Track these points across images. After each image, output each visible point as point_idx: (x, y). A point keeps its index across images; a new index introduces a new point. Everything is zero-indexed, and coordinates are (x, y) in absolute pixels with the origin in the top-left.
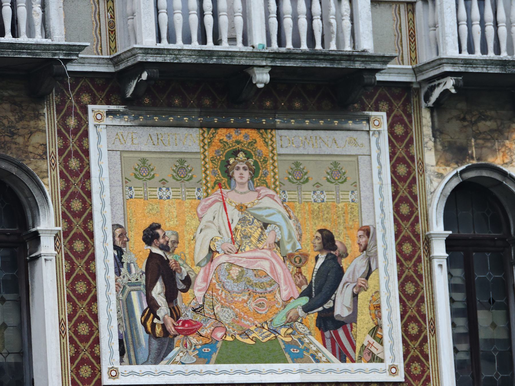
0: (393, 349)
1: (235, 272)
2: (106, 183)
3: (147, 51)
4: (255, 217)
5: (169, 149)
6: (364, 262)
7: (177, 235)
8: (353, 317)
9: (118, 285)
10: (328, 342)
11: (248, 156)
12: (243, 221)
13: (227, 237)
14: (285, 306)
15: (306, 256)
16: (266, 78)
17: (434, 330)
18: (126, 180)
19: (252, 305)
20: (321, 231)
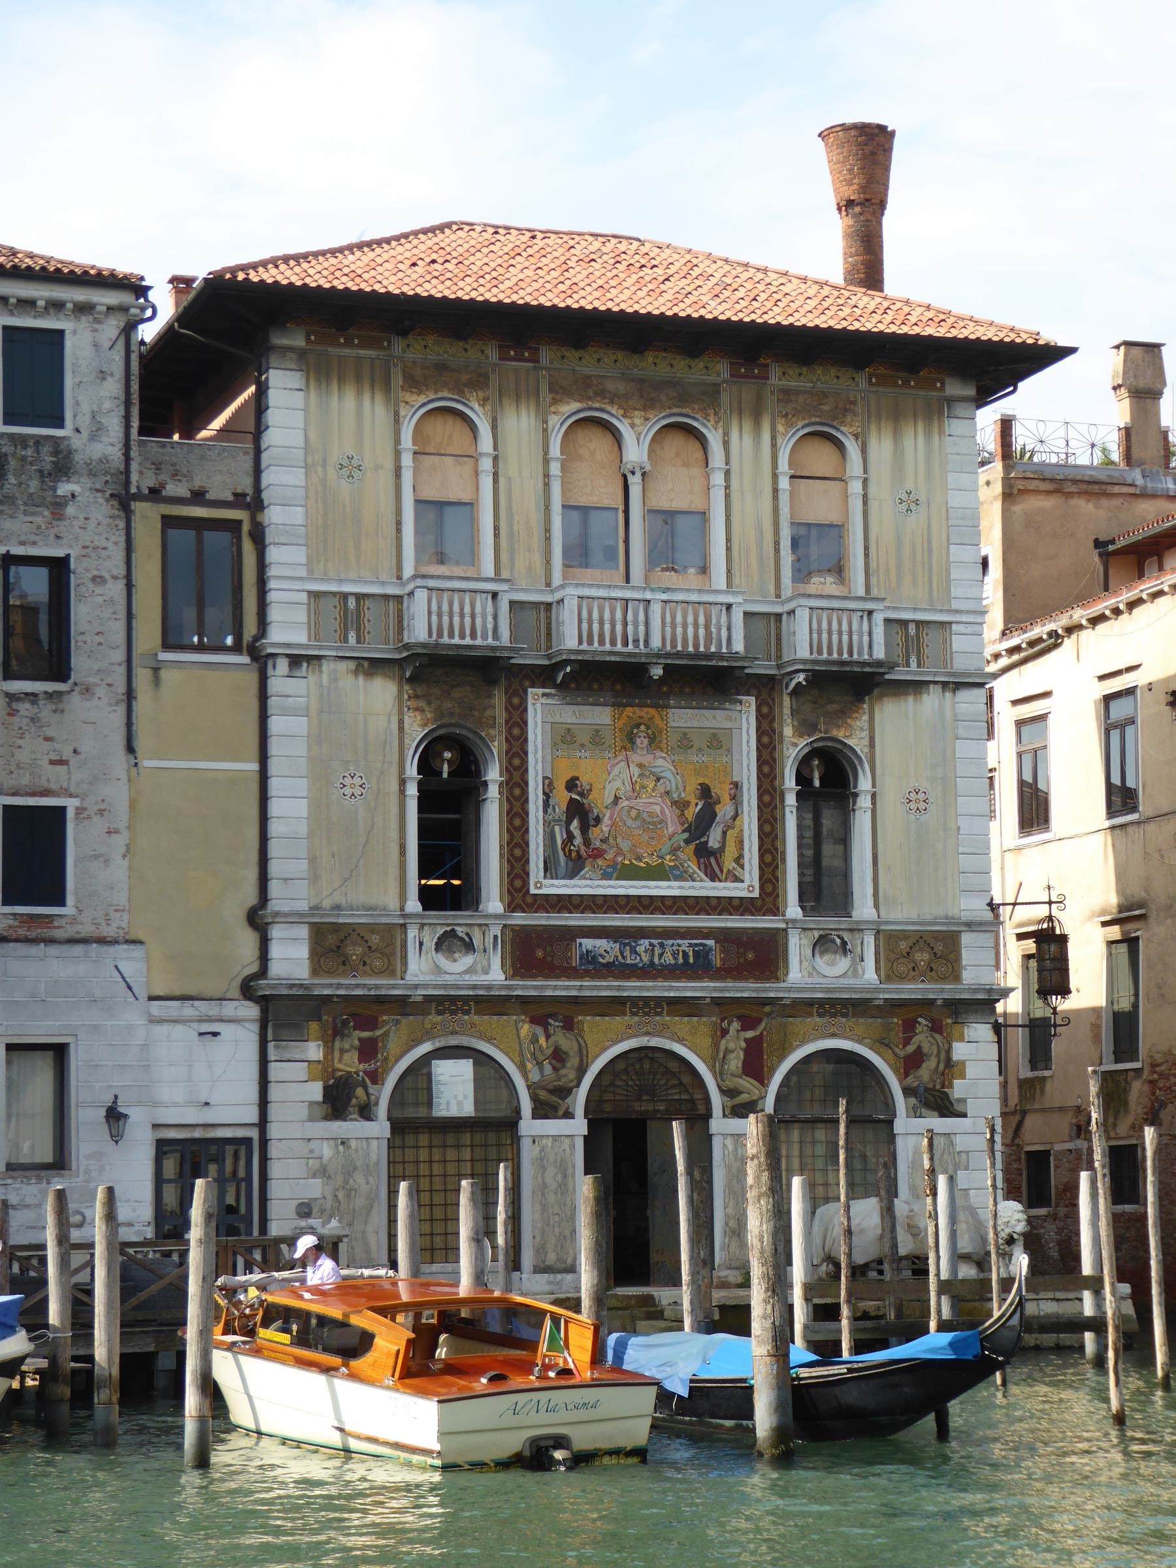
1: (634, 813)
2: (540, 746)
3: (571, 651)
4: (652, 773)
5: (587, 722)
6: (733, 808)
9: (545, 821)
10: (702, 867)
11: (648, 727)
13: (629, 787)
15: (688, 803)
16: (661, 672)
17: (784, 860)
18: (554, 744)
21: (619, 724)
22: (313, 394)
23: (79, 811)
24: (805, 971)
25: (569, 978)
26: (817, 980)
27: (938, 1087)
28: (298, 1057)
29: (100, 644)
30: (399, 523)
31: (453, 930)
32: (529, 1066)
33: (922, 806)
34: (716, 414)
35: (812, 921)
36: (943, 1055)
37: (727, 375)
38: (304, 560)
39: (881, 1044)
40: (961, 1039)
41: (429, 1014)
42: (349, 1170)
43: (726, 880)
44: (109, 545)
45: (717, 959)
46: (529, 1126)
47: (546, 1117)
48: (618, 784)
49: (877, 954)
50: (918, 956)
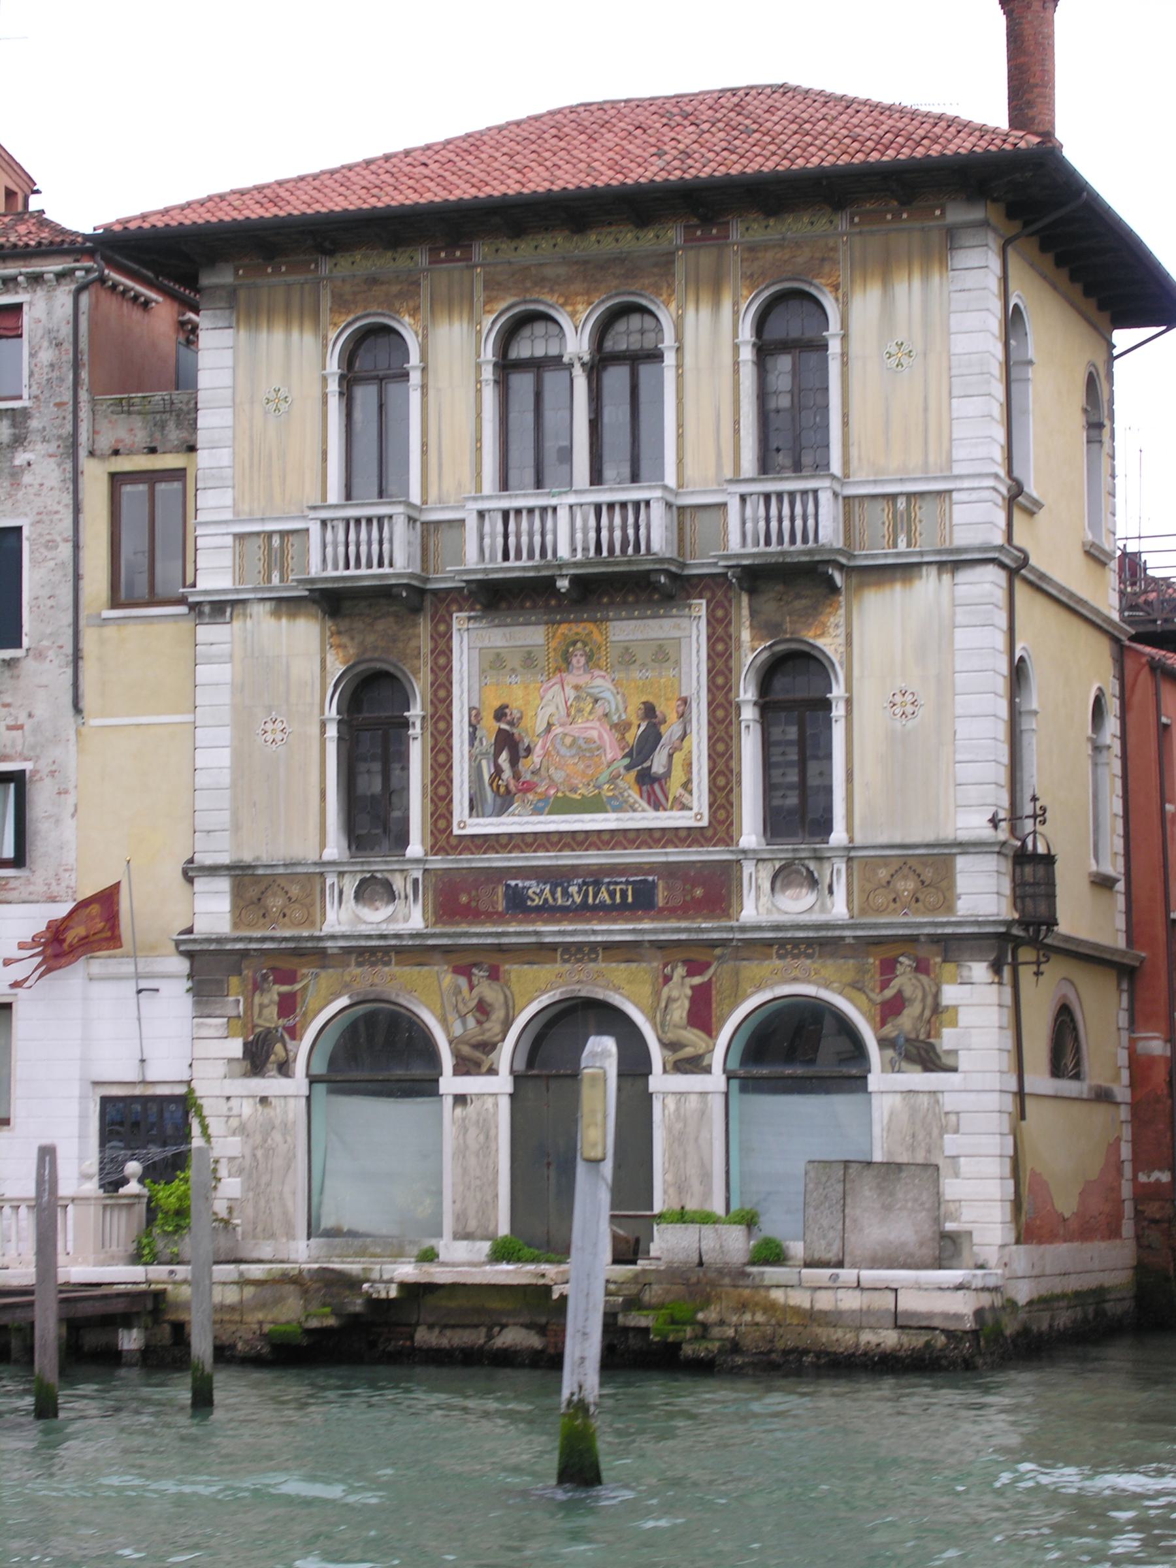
0: (700, 799)
1: (568, 740)
2: (466, 675)
4: (588, 694)
5: (519, 643)
6: (681, 727)
7: (522, 713)
8: (668, 774)
10: (645, 795)
11: (585, 644)
12: (577, 698)
13: (563, 711)
14: (609, 767)
15: (627, 726)
18: (483, 672)
19: (581, 766)
20: (644, 703)
21: (553, 645)
22: (242, 332)
24: (759, 906)
25: (495, 923)
26: (777, 918)
27: (922, 1037)
28: (218, 1012)
29: (52, 607)
31: (373, 877)
32: (450, 1018)
33: (909, 709)
34: (669, 286)
36: (929, 1000)
37: (680, 241)
38: (229, 502)
39: (856, 987)
40: (953, 981)
41: (348, 965)
42: (268, 1128)
43: (672, 809)
44: (60, 508)
45: (661, 899)
46: (450, 1083)
47: (468, 1073)
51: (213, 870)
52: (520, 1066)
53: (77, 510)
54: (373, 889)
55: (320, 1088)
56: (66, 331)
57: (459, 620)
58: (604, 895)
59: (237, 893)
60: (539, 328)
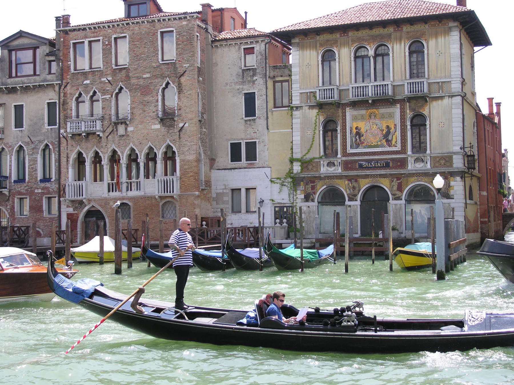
8: (392, 140)
15: (383, 130)
18: (353, 120)
23: (259, 142)
30: (318, 76)
35: (413, 155)
37: (393, 31)
42: (310, 212)
46: (347, 203)
48: (367, 127)
49: (431, 161)
50: (441, 161)
51: (297, 160)
52: (361, 199)
53: (267, 88)
54: (331, 164)
55: (320, 204)
56: (264, 52)
57: (348, 109)
58: (379, 164)
59: (301, 166)
60: (363, 49)
